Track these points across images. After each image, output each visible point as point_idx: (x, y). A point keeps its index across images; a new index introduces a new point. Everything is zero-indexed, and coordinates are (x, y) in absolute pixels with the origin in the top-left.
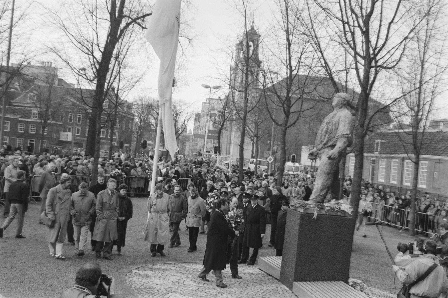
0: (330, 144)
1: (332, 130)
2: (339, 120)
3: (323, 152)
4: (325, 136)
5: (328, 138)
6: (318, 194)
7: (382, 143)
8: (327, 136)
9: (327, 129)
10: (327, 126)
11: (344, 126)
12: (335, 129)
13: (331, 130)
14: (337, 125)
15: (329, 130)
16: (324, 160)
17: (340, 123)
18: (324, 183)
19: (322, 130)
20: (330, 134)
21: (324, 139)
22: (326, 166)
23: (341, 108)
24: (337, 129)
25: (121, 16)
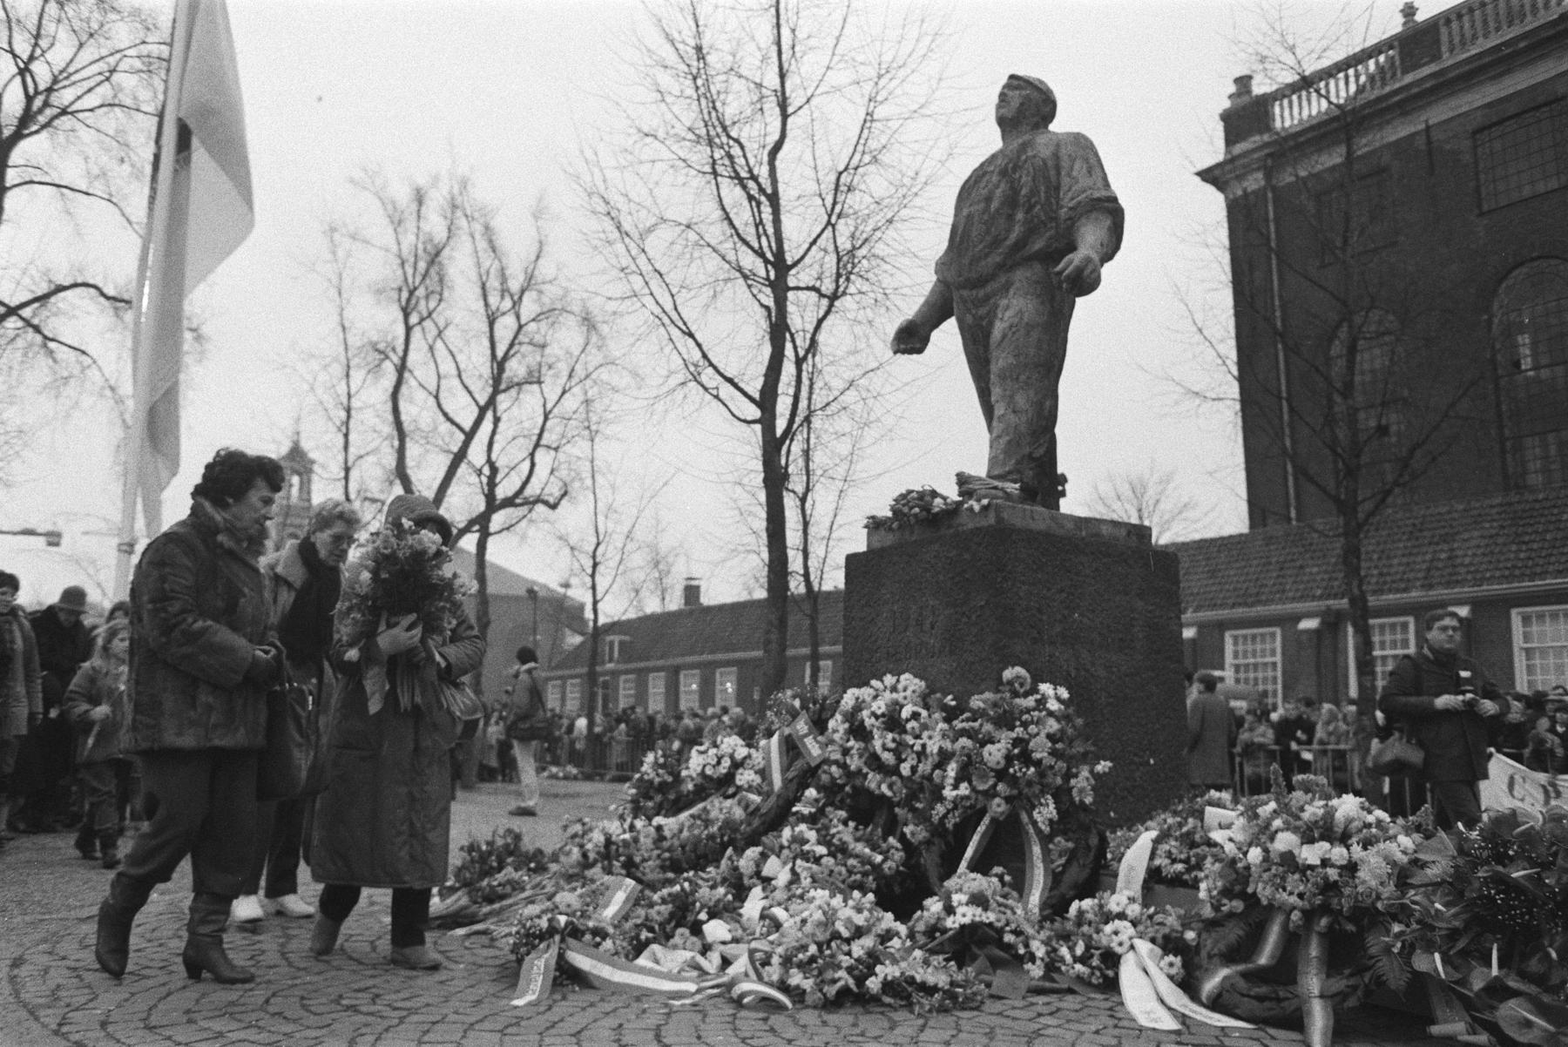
0: (1038, 245)
1: (1034, 192)
3: (1006, 288)
4: (1011, 217)
5: (1026, 222)
6: (1027, 450)
7: (621, 643)
8: (1020, 216)
9: (1014, 190)
12: (1048, 187)
14: (1052, 172)
15: (1023, 192)
17: (1065, 163)
19: (988, 199)
22: (1035, 335)
24: (1058, 188)
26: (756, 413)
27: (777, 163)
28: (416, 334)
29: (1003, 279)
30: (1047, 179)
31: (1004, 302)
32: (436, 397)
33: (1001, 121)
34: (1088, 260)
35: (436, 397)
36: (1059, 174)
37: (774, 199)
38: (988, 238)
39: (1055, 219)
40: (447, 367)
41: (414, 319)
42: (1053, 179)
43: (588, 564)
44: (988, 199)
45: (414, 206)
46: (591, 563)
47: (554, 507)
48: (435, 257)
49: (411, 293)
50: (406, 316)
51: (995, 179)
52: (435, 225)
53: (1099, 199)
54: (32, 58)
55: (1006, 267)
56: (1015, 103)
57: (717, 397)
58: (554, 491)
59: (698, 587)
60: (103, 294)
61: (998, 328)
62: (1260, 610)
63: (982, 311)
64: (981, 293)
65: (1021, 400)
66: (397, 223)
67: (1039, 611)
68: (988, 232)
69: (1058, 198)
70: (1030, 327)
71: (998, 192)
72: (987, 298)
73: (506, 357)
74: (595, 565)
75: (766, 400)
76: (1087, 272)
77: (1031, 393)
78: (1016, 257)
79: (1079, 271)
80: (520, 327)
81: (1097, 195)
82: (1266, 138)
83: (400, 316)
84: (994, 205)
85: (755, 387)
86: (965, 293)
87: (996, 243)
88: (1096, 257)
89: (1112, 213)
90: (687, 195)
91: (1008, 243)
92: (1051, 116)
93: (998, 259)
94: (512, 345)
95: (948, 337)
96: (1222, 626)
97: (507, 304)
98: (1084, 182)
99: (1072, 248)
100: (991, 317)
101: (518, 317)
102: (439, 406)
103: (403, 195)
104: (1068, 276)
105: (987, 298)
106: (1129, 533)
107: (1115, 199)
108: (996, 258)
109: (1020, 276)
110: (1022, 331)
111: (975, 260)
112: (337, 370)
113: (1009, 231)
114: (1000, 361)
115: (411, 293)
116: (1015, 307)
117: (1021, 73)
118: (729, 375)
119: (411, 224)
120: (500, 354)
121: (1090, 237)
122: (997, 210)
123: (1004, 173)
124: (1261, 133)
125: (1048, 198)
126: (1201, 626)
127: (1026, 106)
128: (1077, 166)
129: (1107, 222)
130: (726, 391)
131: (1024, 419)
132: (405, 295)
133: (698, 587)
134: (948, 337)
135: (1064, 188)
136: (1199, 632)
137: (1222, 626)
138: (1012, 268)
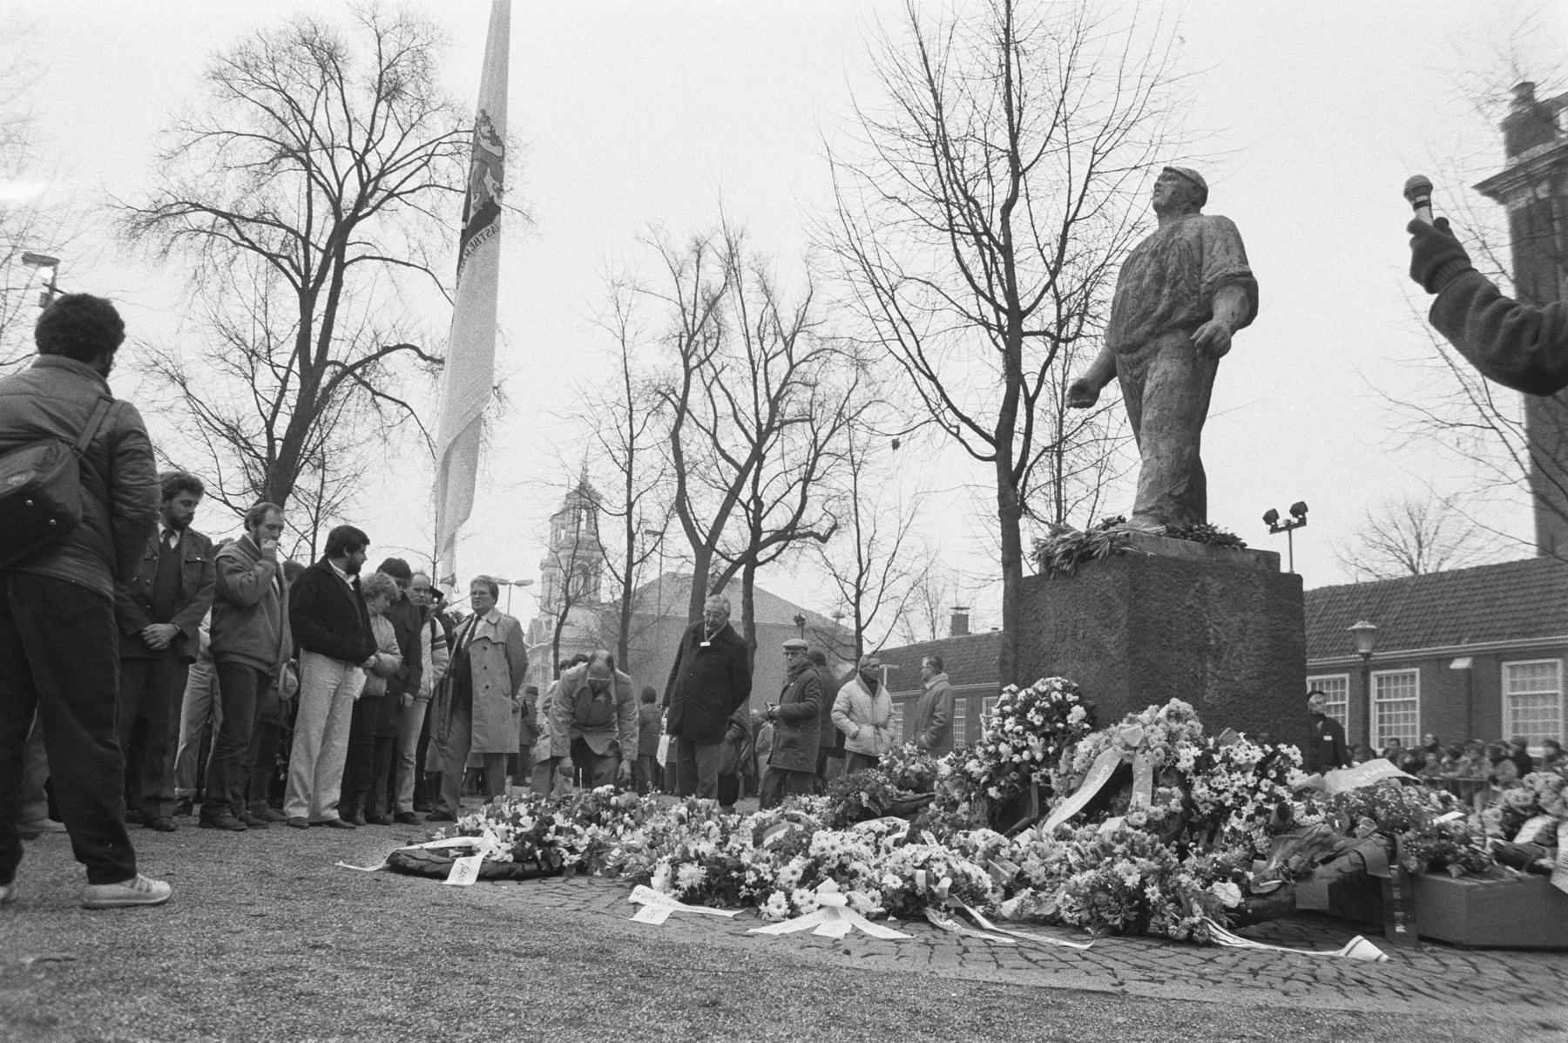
0: (1181, 315)
2: (1200, 237)
4: (1159, 292)
8: (1166, 291)
9: (1162, 270)
10: (1160, 262)
11: (1227, 251)
13: (1177, 271)
14: (1196, 253)
16: (1165, 373)
17: (1207, 245)
19: (1140, 277)
20: (1176, 284)
22: (1177, 393)
23: (1187, 211)
24: (1200, 265)
26: (990, 450)
27: (1011, 219)
28: (695, 377)
29: (1151, 346)
30: (1191, 258)
31: (1153, 365)
32: (714, 436)
33: (1156, 207)
34: (1217, 329)
35: (714, 436)
36: (1201, 253)
37: (1007, 250)
38: (1139, 312)
39: (1198, 292)
40: (724, 406)
41: (693, 362)
42: (1197, 259)
43: (852, 592)
44: (1140, 277)
45: (694, 257)
46: (854, 592)
47: (824, 539)
48: (712, 304)
49: (691, 338)
50: (686, 358)
51: (1147, 259)
52: (713, 274)
54: (366, 151)
56: (1168, 192)
57: (957, 435)
58: (823, 527)
59: (966, 616)
60: (421, 355)
61: (1149, 386)
62: (1540, 640)
63: (1136, 372)
64: (1135, 357)
65: (1162, 447)
66: (678, 275)
67: (1169, 623)
68: (1139, 306)
69: (1200, 275)
70: (1175, 385)
71: (1149, 272)
72: (1140, 361)
73: (779, 397)
74: (859, 594)
75: (1002, 439)
76: (1217, 338)
77: (1173, 441)
78: (1164, 325)
79: (1209, 340)
80: (792, 367)
81: (1232, 271)
82: (1550, 147)
83: (681, 362)
84: (1147, 280)
85: (991, 425)
86: (1123, 356)
88: (1226, 327)
89: (1248, 287)
90: (927, 255)
92: (1203, 200)
93: (1148, 328)
94: (784, 384)
95: (1112, 391)
96: (1500, 656)
97: (780, 345)
98: (1221, 260)
99: (1209, 316)
100: (1143, 377)
101: (790, 357)
102: (716, 444)
103: (684, 250)
104: (1200, 345)
105: (1140, 361)
106: (1258, 559)
107: (1250, 274)
108: (1146, 327)
109: (1168, 342)
110: (1167, 390)
111: (1131, 328)
112: (622, 411)
113: (1156, 304)
114: (1147, 417)
115: (691, 338)
116: (1163, 369)
117: (1173, 166)
118: (965, 414)
119: (690, 272)
120: (773, 394)
121: (1224, 307)
122: (1148, 287)
123: (1154, 254)
124: (1544, 142)
125: (1191, 274)
126: (1477, 657)
127: (1182, 193)
128: (1217, 246)
129: (1240, 294)
130: (966, 432)
132: (685, 340)
133: (966, 616)
134: (1112, 391)
135: (1205, 266)
136: (1474, 663)
137: (1500, 656)
138: (1159, 336)
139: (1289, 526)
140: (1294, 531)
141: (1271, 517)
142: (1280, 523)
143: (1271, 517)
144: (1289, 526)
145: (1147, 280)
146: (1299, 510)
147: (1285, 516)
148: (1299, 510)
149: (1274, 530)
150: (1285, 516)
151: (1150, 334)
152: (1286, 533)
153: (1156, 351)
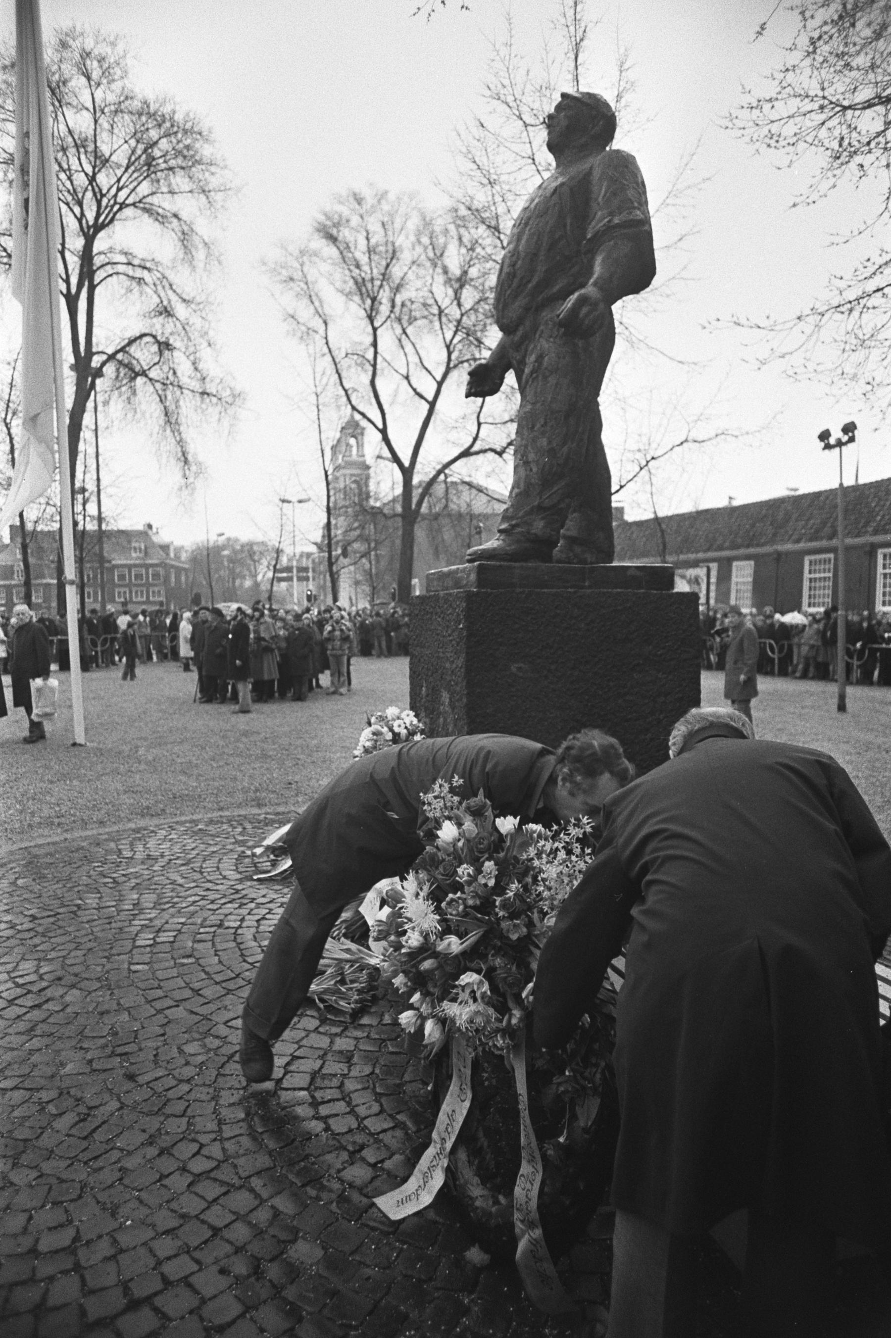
18: (552, 452)
21: (532, 271)
22: (552, 380)
25: (90, 353)
53: (617, 226)
55: (534, 309)
59: (622, 508)
87: (522, 285)
91: (530, 285)
131: (535, 469)
133: (622, 508)
139: (840, 444)
140: (844, 448)
141: (824, 436)
142: (832, 441)
143: (824, 436)
144: (840, 444)
145: (523, 241)
146: (849, 429)
147: (836, 434)
148: (849, 429)
149: (828, 447)
150: (836, 434)
151: (527, 309)
152: (837, 450)
153: (535, 328)
